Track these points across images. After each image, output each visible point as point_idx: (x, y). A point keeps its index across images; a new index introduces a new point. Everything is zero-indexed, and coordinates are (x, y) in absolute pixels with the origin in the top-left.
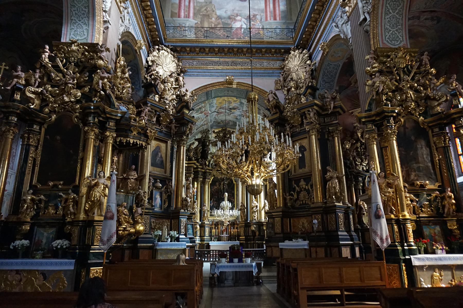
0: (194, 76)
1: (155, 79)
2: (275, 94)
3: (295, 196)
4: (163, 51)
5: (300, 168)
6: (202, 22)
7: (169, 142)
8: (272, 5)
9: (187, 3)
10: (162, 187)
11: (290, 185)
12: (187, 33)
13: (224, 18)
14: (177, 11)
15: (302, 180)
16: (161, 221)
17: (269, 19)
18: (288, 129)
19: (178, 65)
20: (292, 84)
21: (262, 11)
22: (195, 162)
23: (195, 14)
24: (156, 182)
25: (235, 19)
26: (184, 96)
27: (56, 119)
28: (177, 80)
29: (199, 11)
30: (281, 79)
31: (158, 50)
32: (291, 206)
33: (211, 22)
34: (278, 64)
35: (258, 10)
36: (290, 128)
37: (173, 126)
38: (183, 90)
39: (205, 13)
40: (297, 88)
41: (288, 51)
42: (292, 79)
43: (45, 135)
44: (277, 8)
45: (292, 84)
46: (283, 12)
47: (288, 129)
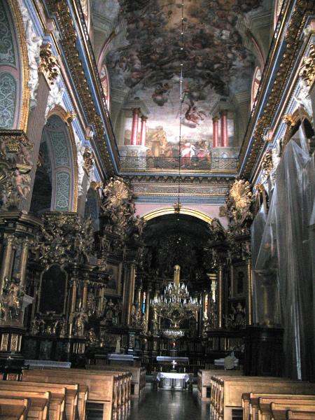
0: (144, 201)
1: (109, 212)
2: (218, 221)
3: (233, 317)
4: (117, 181)
5: (239, 292)
6: (153, 149)
7: (121, 265)
8: (220, 131)
9: (139, 131)
10: (114, 306)
11: (230, 307)
12: (140, 163)
13: (174, 144)
14: (129, 138)
15: (239, 304)
16: (113, 335)
17: (216, 145)
18: (230, 255)
19: (129, 193)
20: (234, 213)
21: (210, 137)
22: (144, 272)
23: (146, 140)
24: (109, 301)
25: (184, 146)
26: (136, 221)
27: (50, 269)
28: (128, 206)
29: (151, 137)
30: (225, 205)
31: (113, 180)
32: (229, 326)
33: (162, 149)
34: (224, 190)
35: (207, 136)
36: (232, 254)
37: (124, 250)
38: (135, 215)
39: (156, 139)
40: (239, 217)
41: (233, 179)
42: (235, 209)
43: (43, 279)
44: (225, 135)
45: (234, 213)
46: (230, 138)
47: (230, 255)
